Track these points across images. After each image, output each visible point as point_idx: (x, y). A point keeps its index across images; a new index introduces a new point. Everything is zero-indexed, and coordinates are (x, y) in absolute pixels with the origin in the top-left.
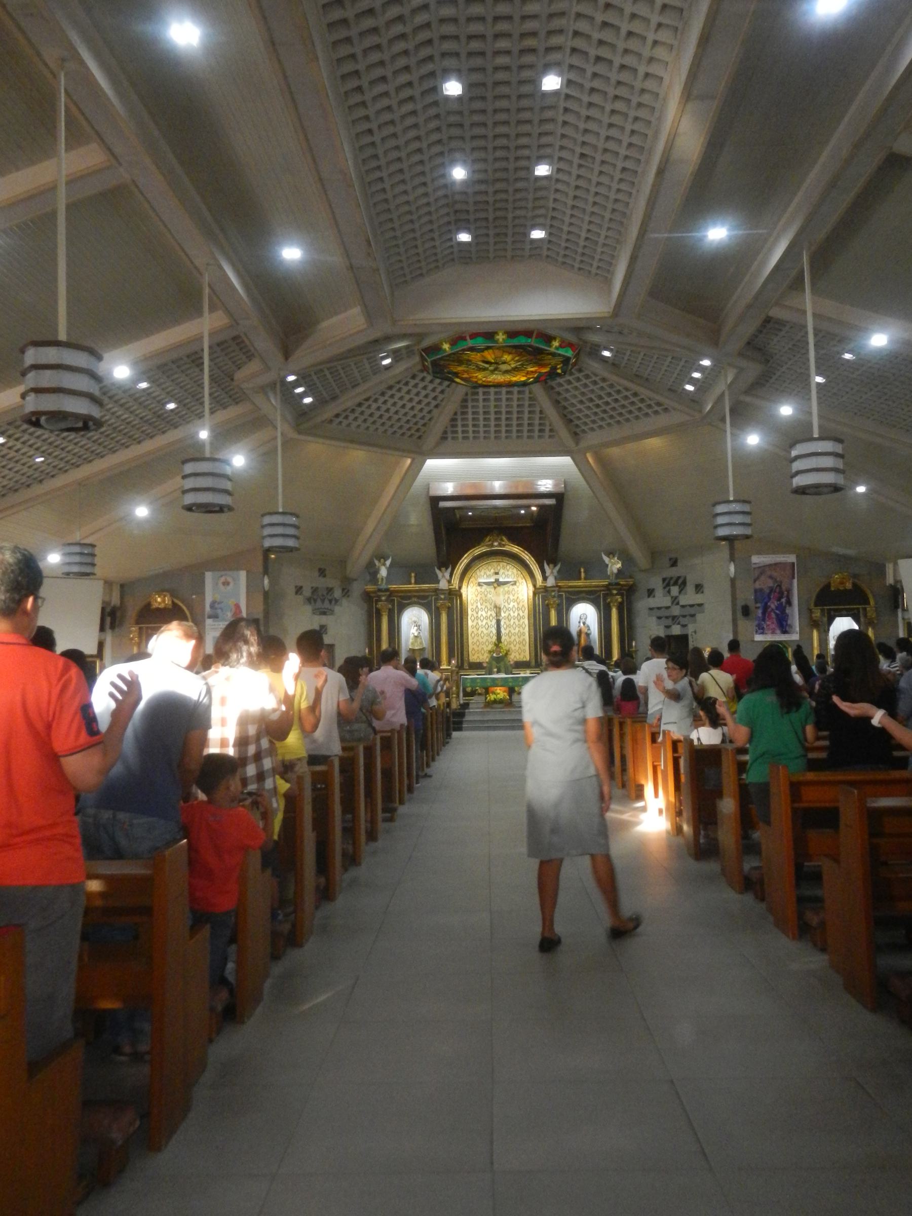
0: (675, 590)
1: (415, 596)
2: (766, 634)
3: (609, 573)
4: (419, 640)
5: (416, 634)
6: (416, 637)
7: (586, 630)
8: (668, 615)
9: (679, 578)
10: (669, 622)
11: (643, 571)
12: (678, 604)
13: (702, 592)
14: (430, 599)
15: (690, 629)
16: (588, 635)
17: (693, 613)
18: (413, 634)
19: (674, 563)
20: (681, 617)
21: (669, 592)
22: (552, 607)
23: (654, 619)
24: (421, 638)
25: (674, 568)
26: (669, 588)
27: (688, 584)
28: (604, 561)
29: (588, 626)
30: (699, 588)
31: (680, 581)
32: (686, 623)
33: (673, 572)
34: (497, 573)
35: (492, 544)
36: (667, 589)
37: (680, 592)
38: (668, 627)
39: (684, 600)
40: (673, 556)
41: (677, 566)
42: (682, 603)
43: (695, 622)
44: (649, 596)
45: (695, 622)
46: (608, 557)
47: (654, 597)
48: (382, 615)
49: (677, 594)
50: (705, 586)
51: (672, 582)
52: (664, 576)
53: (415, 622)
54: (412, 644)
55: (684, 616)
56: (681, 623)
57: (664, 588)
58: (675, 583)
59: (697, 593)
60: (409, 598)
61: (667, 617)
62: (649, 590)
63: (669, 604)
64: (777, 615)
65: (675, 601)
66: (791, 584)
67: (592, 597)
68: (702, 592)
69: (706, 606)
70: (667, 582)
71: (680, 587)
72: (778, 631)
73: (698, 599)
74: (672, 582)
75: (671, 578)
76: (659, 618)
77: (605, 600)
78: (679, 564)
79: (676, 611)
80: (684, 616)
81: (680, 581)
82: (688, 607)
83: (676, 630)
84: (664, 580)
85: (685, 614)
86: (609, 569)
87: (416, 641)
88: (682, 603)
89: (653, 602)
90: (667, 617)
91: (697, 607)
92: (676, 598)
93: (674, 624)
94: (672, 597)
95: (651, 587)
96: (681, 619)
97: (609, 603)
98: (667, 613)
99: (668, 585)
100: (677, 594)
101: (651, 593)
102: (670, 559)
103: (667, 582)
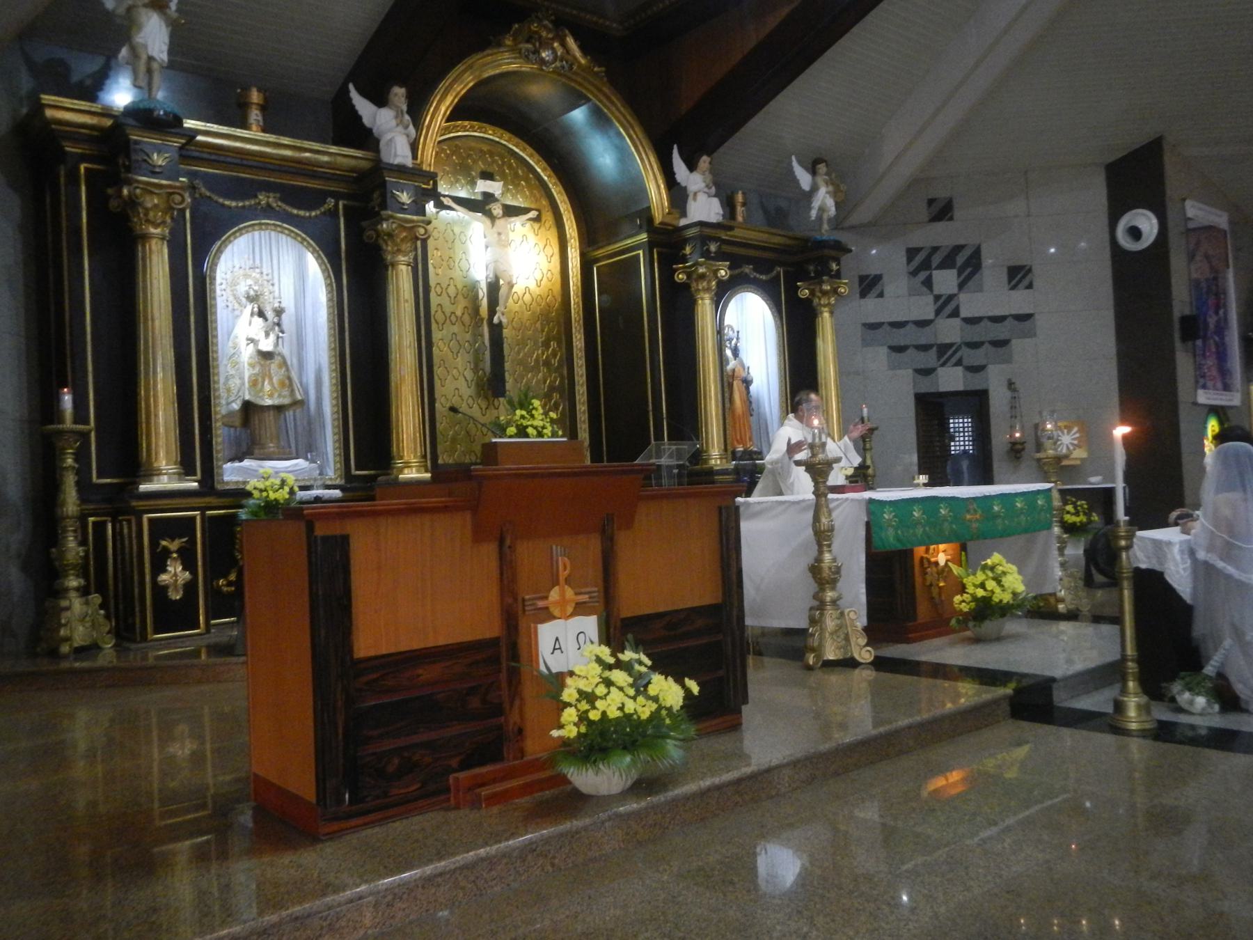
0: (946, 280)
1: (268, 187)
2: (1208, 389)
3: (814, 213)
4: (274, 366)
5: (267, 345)
6: (267, 356)
7: (744, 375)
8: (923, 341)
9: (958, 249)
10: (930, 359)
11: (842, 229)
12: (955, 313)
13: (1030, 286)
14: (331, 202)
15: (995, 382)
16: (747, 382)
17: (1002, 337)
18: (251, 341)
19: (942, 211)
20: (964, 348)
21: (928, 283)
22: (708, 290)
23: (883, 351)
24: (284, 363)
25: (940, 226)
26: (928, 273)
27: (987, 262)
28: (795, 181)
29: (743, 365)
30: (1018, 275)
31: (960, 259)
32: (984, 362)
33: (942, 235)
34: (487, 176)
35: (537, 52)
36: (923, 275)
37: (961, 286)
38: (926, 372)
39: (971, 305)
40: (941, 193)
41: (951, 219)
42: (964, 313)
43: (1008, 360)
44: (863, 294)
45: (1008, 360)
46: (814, 172)
47: (881, 295)
48: (145, 237)
49: (955, 291)
50: (1037, 270)
51: (936, 260)
52: (914, 244)
53: (252, 299)
54: (254, 383)
55: (974, 345)
56: (965, 362)
57: (914, 273)
58: (947, 263)
59: (1013, 288)
60: (244, 190)
61: (924, 348)
62: (862, 279)
63: (931, 316)
64: (1217, 345)
65: (946, 305)
66: (1225, 279)
67: (763, 277)
68: (1030, 286)
69: (1041, 322)
70: (919, 258)
71: (959, 275)
72: (1219, 385)
73: (1018, 301)
74: (936, 260)
75: (935, 249)
76: (898, 349)
77: (792, 290)
78: (957, 213)
79: (949, 331)
80: (974, 345)
81: (960, 260)
82: (985, 323)
83: (951, 379)
84: (911, 253)
85: (976, 339)
86: (816, 204)
87: (266, 374)
88: (964, 313)
89: (872, 309)
90: (924, 348)
91: (989, 323)
92: (951, 297)
93: (943, 365)
94: (937, 298)
95: (873, 271)
96: (965, 352)
97: (808, 301)
98: (924, 337)
99: (926, 265)
100: (955, 291)
101: (869, 285)
102: (931, 202)
103: (919, 258)
